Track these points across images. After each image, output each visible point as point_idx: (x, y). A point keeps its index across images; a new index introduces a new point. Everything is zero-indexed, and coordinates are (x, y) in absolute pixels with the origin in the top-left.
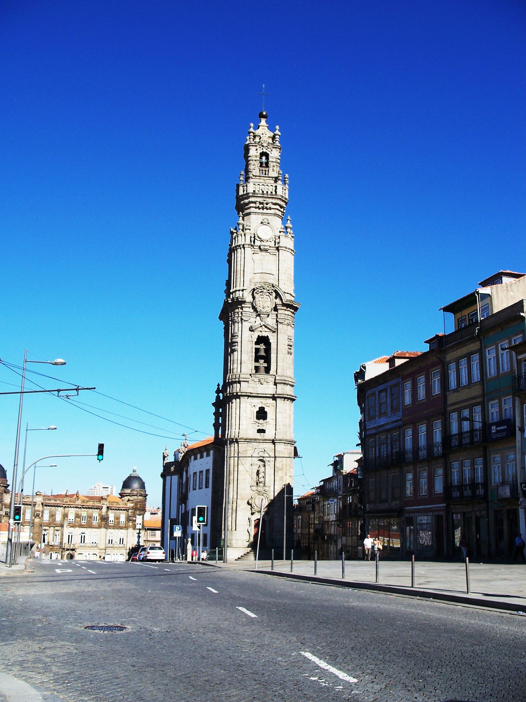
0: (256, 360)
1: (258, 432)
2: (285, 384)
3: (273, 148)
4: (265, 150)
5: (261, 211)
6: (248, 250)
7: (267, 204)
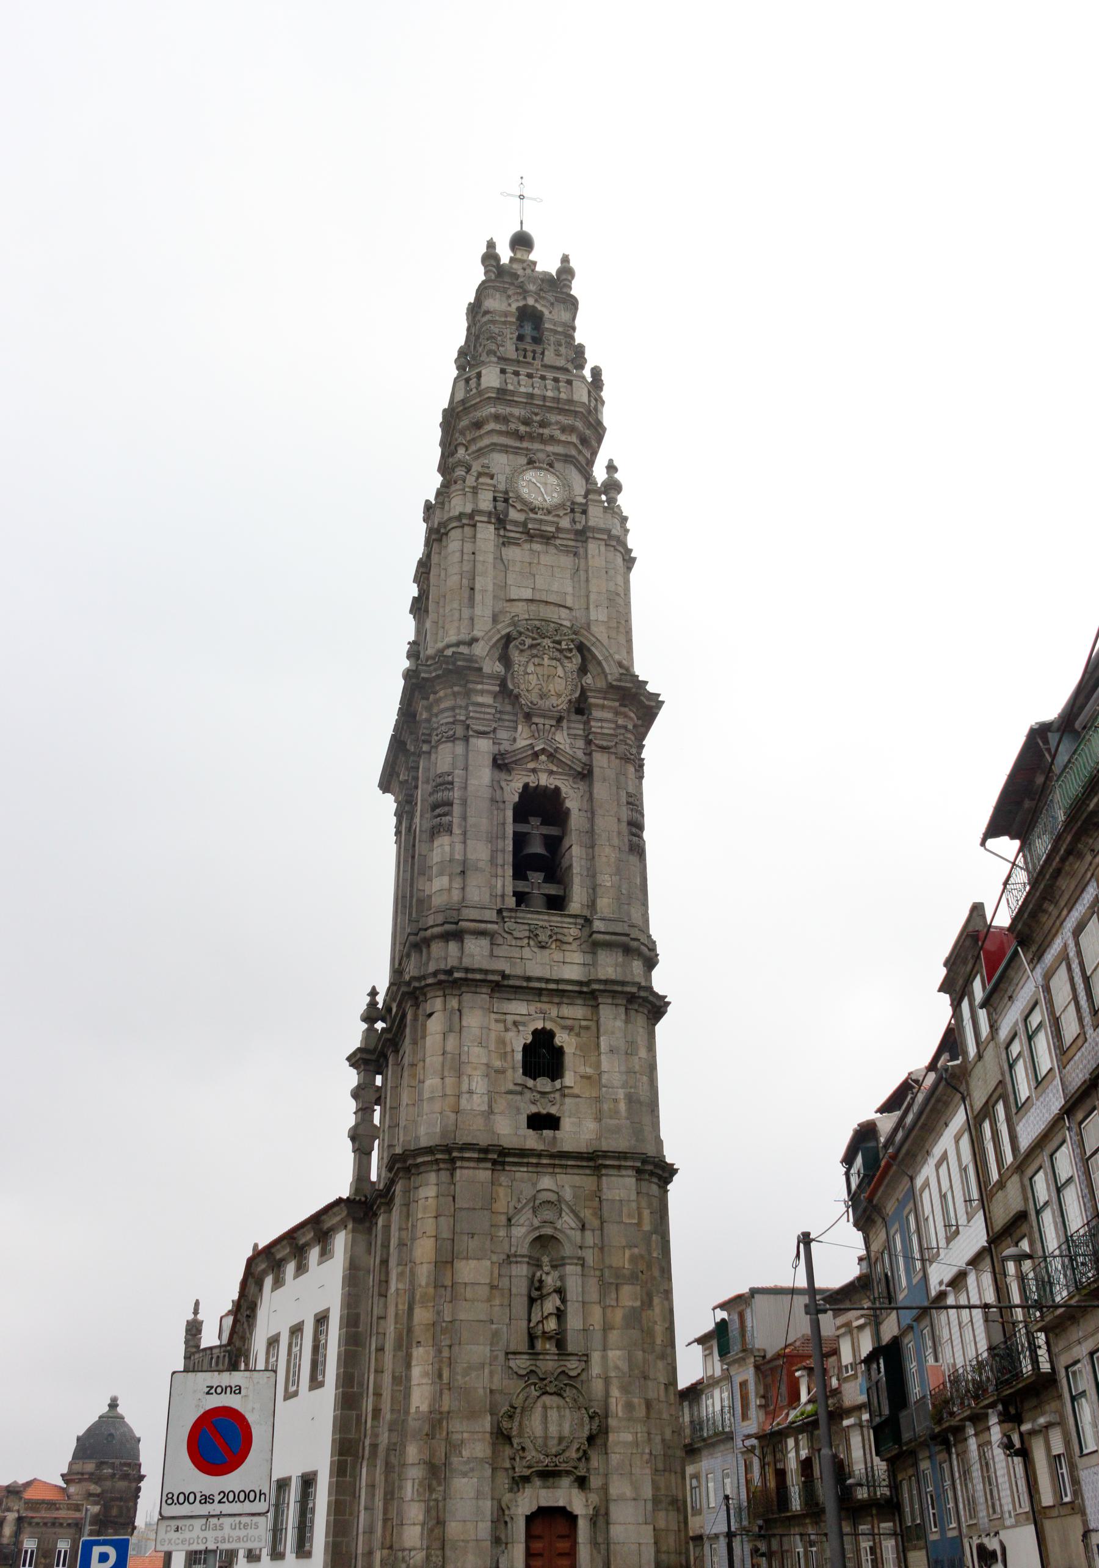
0: (519, 873)
1: (529, 1127)
2: (627, 950)
3: (557, 299)
4: (531, 301)
5: (525, 445)
6: (487, 533)
7: (543, 424)
